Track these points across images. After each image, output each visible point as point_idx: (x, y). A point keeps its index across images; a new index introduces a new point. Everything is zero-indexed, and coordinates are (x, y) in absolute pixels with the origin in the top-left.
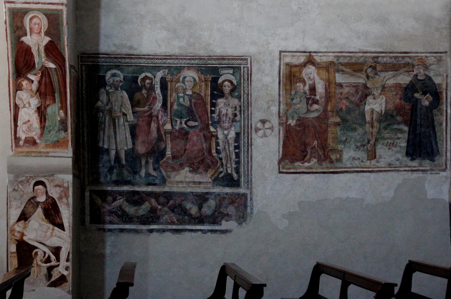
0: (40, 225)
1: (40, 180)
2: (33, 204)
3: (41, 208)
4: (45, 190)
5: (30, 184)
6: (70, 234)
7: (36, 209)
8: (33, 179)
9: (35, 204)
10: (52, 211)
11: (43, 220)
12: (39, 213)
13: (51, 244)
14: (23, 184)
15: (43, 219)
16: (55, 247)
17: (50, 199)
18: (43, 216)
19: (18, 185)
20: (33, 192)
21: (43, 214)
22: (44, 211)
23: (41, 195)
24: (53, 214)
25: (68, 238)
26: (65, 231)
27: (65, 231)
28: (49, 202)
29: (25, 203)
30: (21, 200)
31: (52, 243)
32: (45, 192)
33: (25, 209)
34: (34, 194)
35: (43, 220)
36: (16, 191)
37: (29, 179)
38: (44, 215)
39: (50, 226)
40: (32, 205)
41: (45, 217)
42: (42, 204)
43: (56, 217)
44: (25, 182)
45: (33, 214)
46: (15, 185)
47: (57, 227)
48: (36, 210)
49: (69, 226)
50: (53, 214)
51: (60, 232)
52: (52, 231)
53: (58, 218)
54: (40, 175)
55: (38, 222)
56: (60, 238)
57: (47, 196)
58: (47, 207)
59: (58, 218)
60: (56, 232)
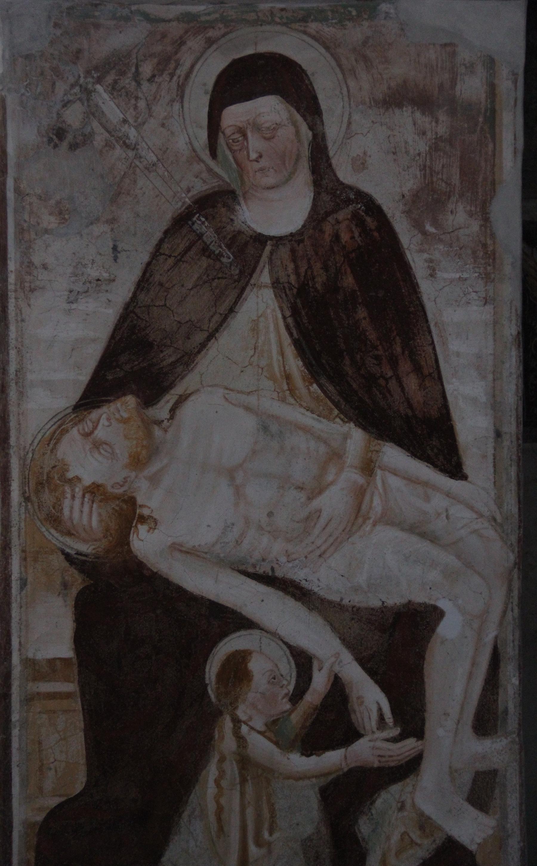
0: (265, 429)
1: (263, 48)
2: (206, 251)
3: (276, 284)
4: (306, 134)
5: (181, 89)
6: (499, 501)
7: (232, 295)
8: (210, 42)
9: (228, 257)
10: (362, 313)
11: (292, 390)
12: (255, 329)
13: (357, 589)
14: (127, 82)
15: (288, 377)
16: (384, 609)
17: (341, 215)
18: (290, 351)
19: (88, 92)
20: (205, 155)
21: (287, 340)
22: (295, 312)
23: (270, 180)
24: (372, 335)
25: (491, 533)
26: (464, 477)
27: (464, 477)
28: (337, 237)
29: (150, 248)
30: (112, 221)
31: (362, 579)
32: (306, 152)
33: (141, 296)
34: (218, 170)
35: (292, 390)
36: (73, 147)
37: (181, 42)
38: (296, 343)
39: (346, 437)
40: (205, 262)
41: (308, 365)
42: (284, 252)
43: (394, 362)
44: (147, 69)
45: (212, 336)
46: (61, 88)
47: (400, 444)
48: (231, 310)
49: (498, 434)
50: (372, 335)
51: (426, 484)
52: (361, 480)
53: (405, 366)
54: (265, 6)
55: (247, 408)
56: (423, 535)
57: (317, 184)
58: (321, 279)
59: (405, 366)
60: (394, 481)
